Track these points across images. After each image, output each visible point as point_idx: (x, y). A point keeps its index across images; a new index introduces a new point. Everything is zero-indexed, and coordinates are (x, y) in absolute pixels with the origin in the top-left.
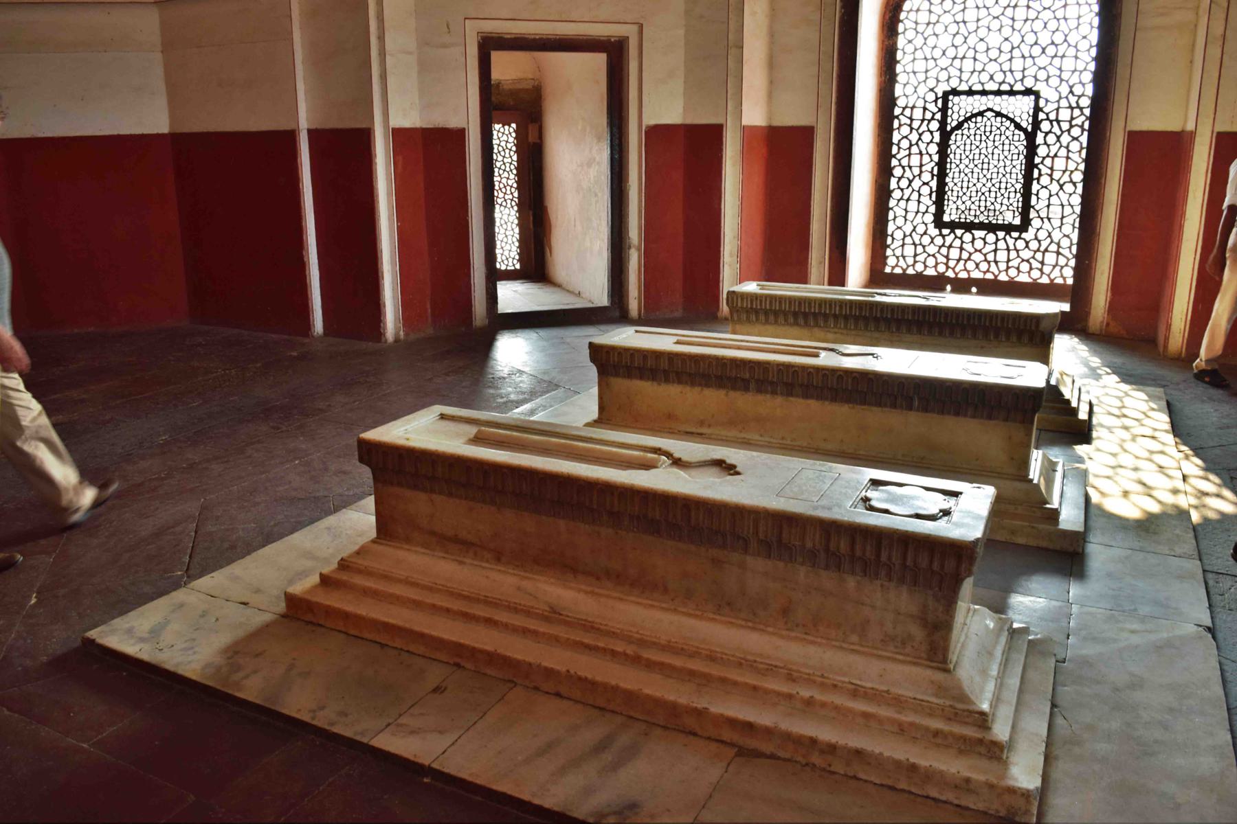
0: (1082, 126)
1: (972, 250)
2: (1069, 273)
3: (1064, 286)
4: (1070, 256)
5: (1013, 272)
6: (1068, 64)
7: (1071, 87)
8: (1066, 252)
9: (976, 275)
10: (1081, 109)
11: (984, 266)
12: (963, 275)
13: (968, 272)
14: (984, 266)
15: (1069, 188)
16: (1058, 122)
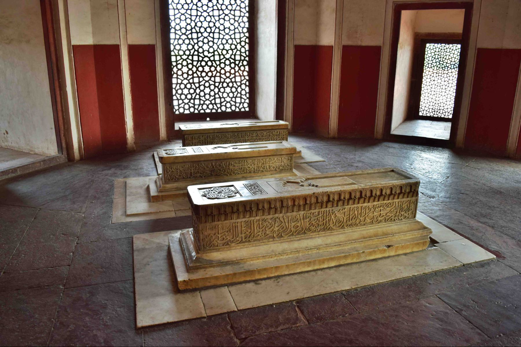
0: (245, 42)
1: (205, 100)
2: (246, 105)
3: (245, 112)
4: (246, 98)
5: (223, 108)
6: (237, 13)
7: (239, 24)
8: (244, 97)
9: (208, 111)
10: (244, 33)
11: (211, 106)
12: (202, 111)
13: (204, 110)
14: (211, 106)
15: (242, 68)
16: (235, 39)
